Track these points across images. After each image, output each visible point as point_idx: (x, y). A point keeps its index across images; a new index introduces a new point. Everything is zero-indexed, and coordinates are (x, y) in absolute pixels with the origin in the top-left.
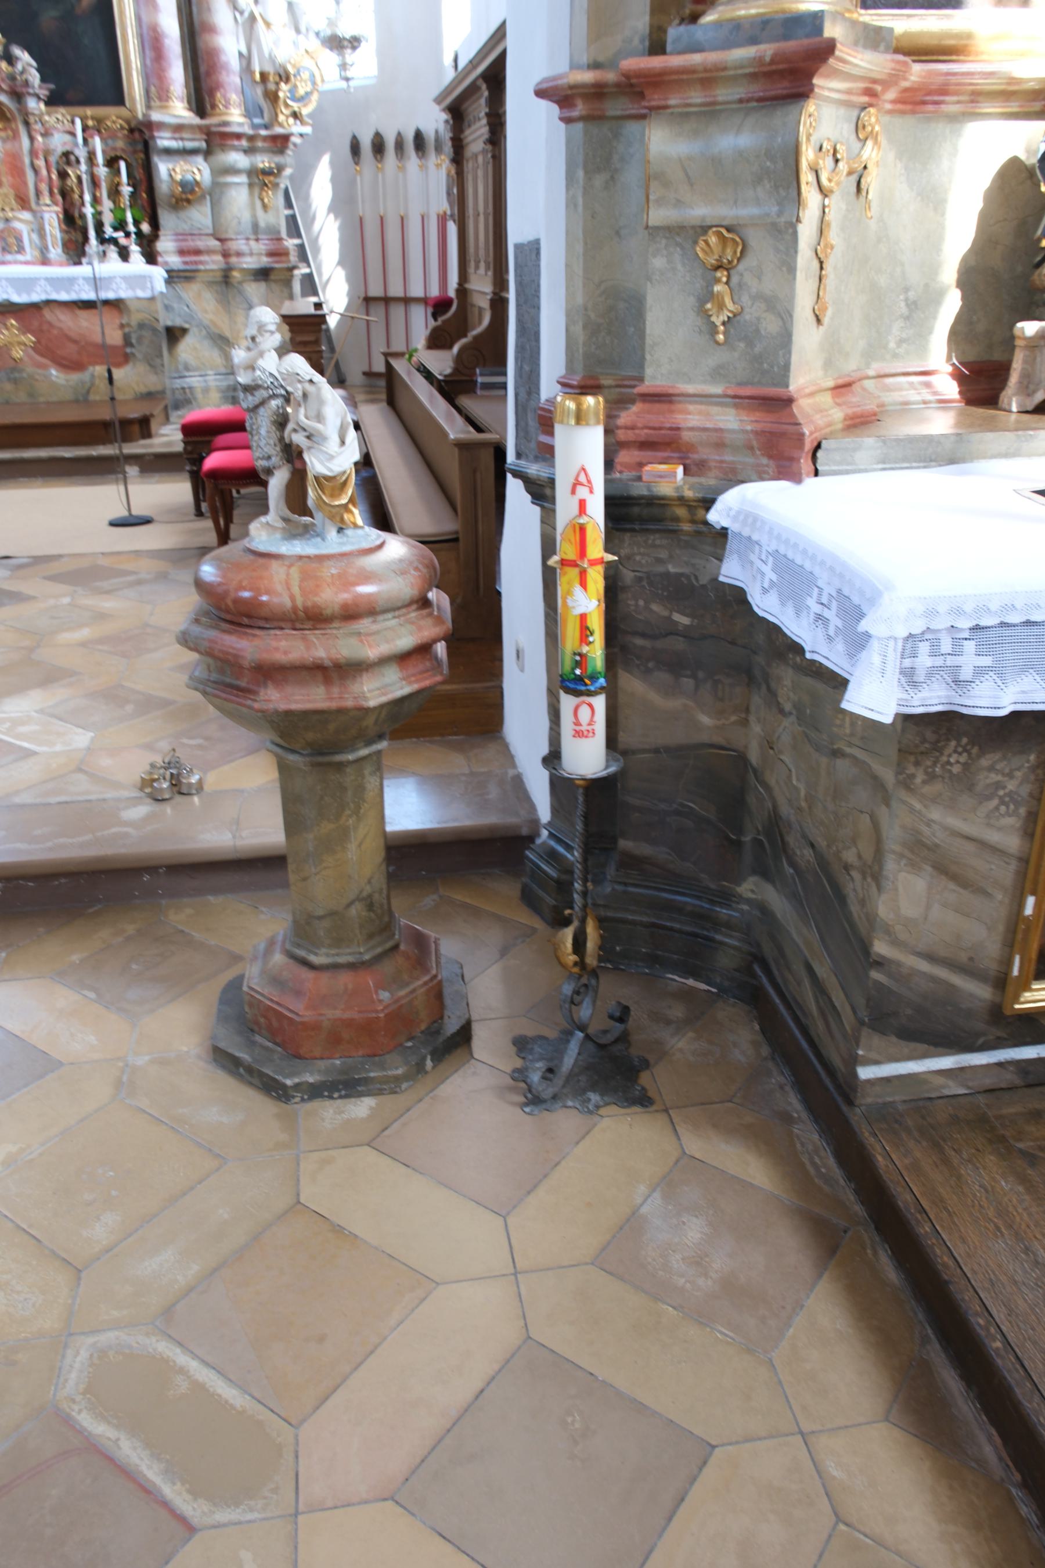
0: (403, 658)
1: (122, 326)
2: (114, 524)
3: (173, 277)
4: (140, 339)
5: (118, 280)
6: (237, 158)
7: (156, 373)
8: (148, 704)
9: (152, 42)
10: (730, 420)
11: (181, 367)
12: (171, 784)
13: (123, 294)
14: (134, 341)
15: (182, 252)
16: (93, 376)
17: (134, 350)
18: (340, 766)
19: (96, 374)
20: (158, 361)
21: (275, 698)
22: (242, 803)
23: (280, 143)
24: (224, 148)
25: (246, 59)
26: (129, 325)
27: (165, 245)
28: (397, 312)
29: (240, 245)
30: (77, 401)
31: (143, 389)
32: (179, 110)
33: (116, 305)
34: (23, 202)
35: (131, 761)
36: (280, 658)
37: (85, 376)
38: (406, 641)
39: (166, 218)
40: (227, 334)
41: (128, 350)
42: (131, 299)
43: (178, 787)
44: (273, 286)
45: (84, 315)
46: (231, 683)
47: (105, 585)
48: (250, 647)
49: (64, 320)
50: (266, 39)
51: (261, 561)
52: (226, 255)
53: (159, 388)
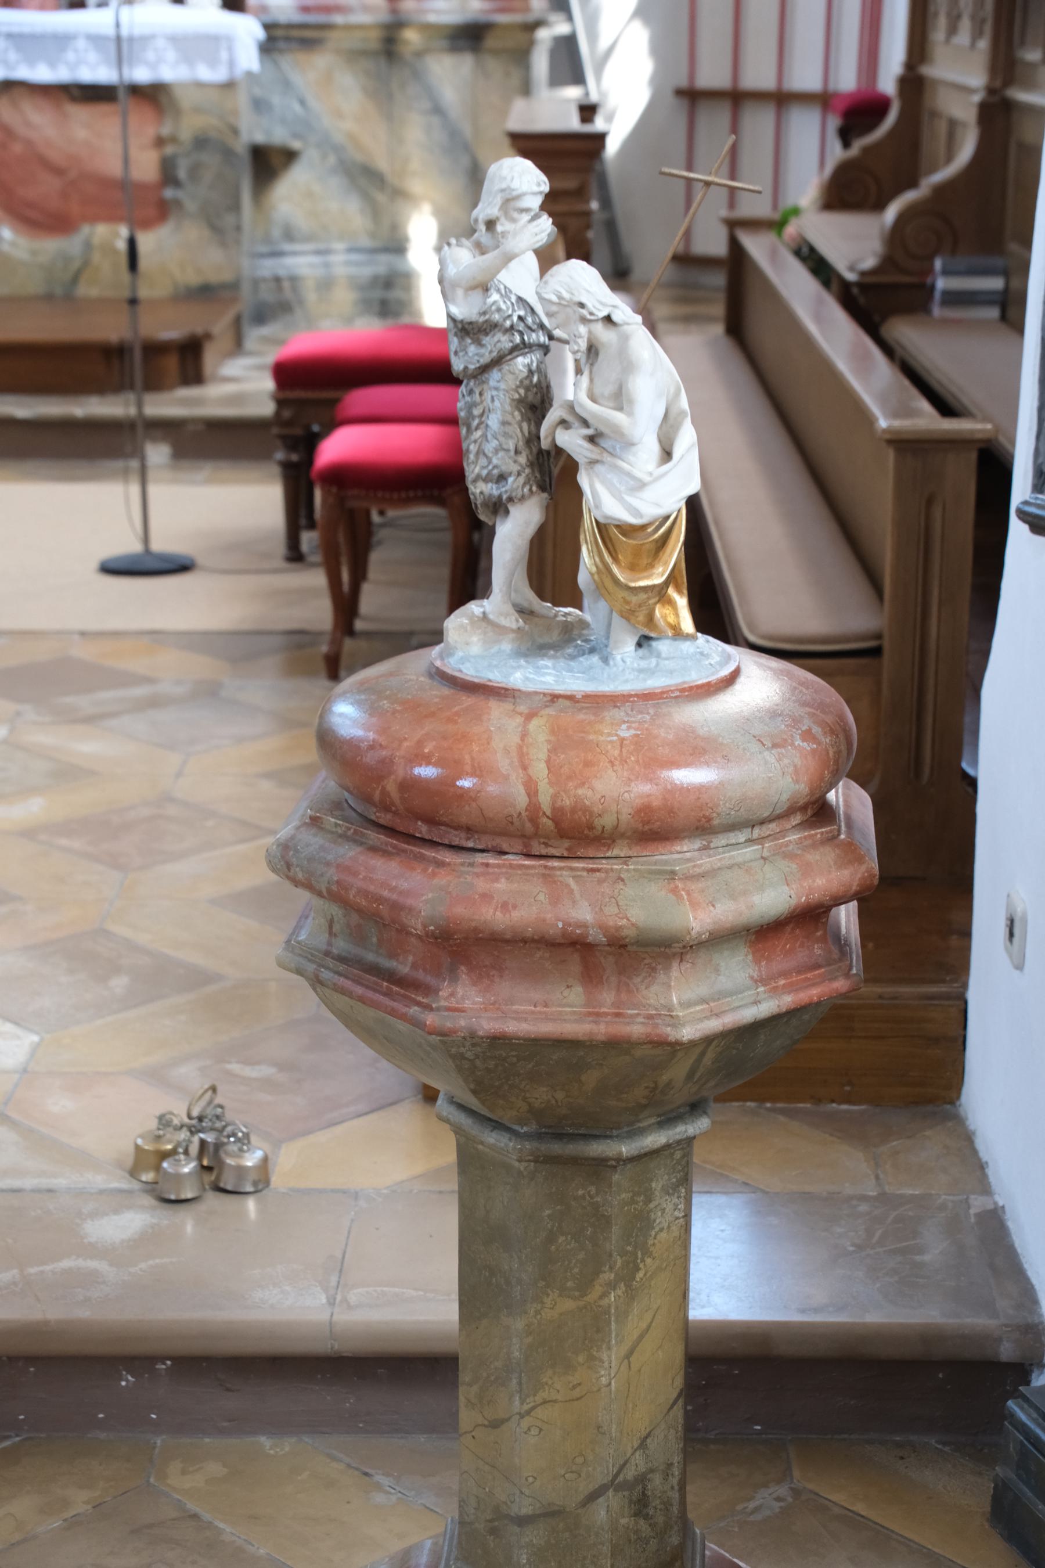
0: (763, 934)
1: (160, 142)
2: (112, 569)
4: (195, 171)
5: (161, 43)
7: (223, 244)
8: (162, 978)
11: (276, 233)
12: (199, 1165)
13: (168, 74)
14: (182, 174)
16: (88, 246)
17: (180, 194)
18: (600, 1167)
19: (96, 240)
20: (229, 220)
21: (474, 1006)
22: (360, 1223)
26: (173, 139)
30: (49, 297)
31: (193, 279)
33: (152, 96)
35: (117, 1113)
36: (492, 917)
37: (72, 245)
38: (773, 896)
40: (382, 164)
41: (169, 193)
42: (184, 85)
43: (216, 1175)
44: (493, 64)
45: (80, 114)
46: (375, 966)
47: (84, 703)
48: (434, 890)
49: (39, 123)
51: (467, 701)
53: (227, 276)
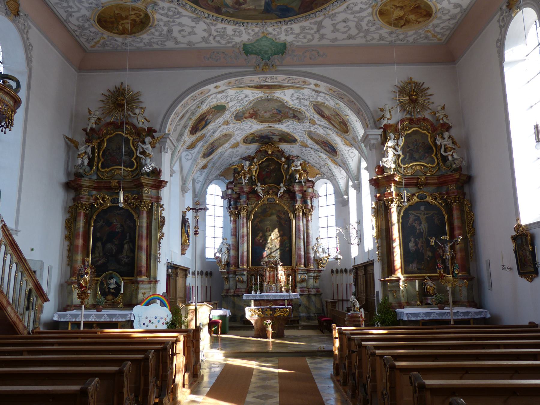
3: (300, 295)
6: (311, 274)
9: (298, 256)
10: (396, 305)
15: (301, 291)
23: (320, 271)
24: (310, 273)
25: (314, 258)
27: (298, 290)
28: (340, 303)
29: (311, 289)
32: (303, 267)
34: (274, 283)
39: (298, 285)
50: (318, 255)
52: (309, 291)
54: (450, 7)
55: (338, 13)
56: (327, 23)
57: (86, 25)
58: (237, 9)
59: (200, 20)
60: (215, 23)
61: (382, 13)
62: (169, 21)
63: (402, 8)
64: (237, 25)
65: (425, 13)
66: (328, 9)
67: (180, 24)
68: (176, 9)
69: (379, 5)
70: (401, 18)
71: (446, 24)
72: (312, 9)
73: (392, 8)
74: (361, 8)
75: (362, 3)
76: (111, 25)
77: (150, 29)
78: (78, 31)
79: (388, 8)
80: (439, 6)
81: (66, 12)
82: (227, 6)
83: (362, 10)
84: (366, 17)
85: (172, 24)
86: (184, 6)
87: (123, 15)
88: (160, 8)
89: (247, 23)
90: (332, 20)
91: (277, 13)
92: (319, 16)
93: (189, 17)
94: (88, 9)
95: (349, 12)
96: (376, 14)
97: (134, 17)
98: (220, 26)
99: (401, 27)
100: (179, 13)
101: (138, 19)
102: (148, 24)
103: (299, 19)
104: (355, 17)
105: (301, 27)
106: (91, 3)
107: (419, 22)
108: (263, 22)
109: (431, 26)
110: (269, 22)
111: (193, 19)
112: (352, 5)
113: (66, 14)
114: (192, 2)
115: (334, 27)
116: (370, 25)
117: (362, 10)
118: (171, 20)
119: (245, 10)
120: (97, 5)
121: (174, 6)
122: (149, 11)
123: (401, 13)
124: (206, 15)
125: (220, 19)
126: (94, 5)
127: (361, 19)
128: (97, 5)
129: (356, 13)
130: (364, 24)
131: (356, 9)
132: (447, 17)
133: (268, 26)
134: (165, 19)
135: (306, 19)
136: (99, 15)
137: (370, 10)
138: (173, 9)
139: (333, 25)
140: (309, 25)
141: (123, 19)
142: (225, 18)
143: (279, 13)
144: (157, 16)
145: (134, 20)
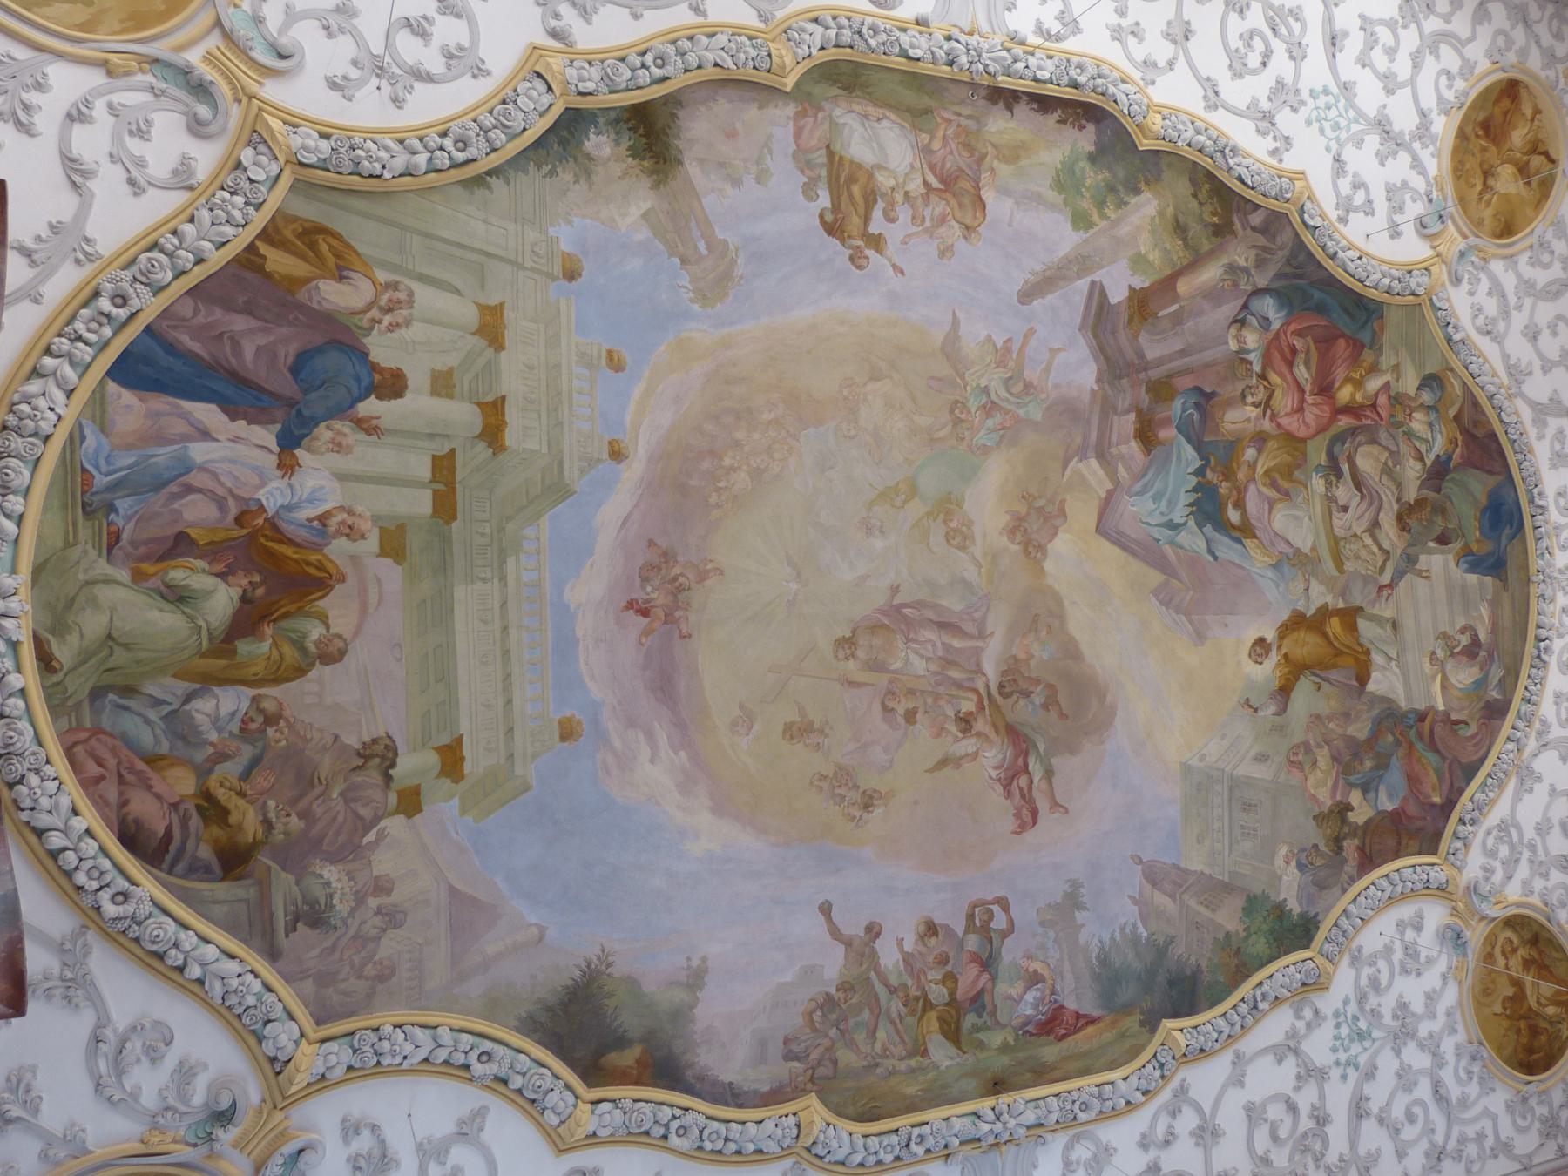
54: (1485, 33)
55: (1506, 357)
56: (1538, 387)
57: (1542, 1111)
58: (1490, 655)
59: (1529, 768)
60: (1537, 725)
61: (1506, 229)
62: (1531, 862)
63: (1487, 174)
64: (1544, 657)
65: (1506, 103)
66: (1492, 389)
67: (1542, 829)
68: (1489, 833)
69: (1478, 241)
70: (1523, 170)
71: (1542, 30)
72: (1493, 436)
73: (1489, 203)
74: (1490, 294)
75: (1472, 294)
76: (1543, 1038)
77: (1559, 924)
78: (1560, 1140)
79: (1488, 213)
80: (1484, 65)
81: (1496, 1157)
82: (1481, 684)
83: (1497, 289)
84: (1518, 275)
85: (1540, 851)
86: (1481, 808)
87: (1510, 991)
88: (1487, 879)
89: (1539, 627)
90: (1530, 373)
91: (1504, 541)
92: (1516, 413)
93: (1517, 798)
94: (1487, 1090)
95: (1501, 325)
96: (1510, 245)
97: (1516, 962)
98: (1547, 708)
99: (1553, 161)
100: (1503, 827)
101: (1522, 952)
102: (1542, 926)
103: (1525, 473)
104: (1519, 308)
105: (1554, 466)
106: (1470, 1073)
107: (1537, 111)
108: (1534, 578)
109: (1551, 74)
110: (1535, 563)
111: (1524, 787)
112: (1480, 321)
113: (1502, 1158)
114: (1468, 783)
115: (1555, 364)
116: (1546, 258)
117: (1497, 289)
118: (1526, 854)
119: (1495, 629)
120: (1474, 1058)
121: (1480, 835)
122: (1495, 912)
123: (1506, 172)
124: (1511, 746)
125: (1525, 708)
126: (1476, 1068)
127: (1527, 286)
128: (1474, 1058)
129: (1507, 305)
130: (1542, 277)
131: (1491, 307)
132: (1519, 35)
133: (1550, 565)
134: (1523, 871)
135: (1525, 452)
136: (1508, 1062)
137: (1497, 266)
138: (1490, 841)
139: (1546, 370)
140: (1546, 443)
141: (1519, 997)
142: (1520, 692)
143: (1507, 531)
144: (1513, 892)
145: (1527, 964)
